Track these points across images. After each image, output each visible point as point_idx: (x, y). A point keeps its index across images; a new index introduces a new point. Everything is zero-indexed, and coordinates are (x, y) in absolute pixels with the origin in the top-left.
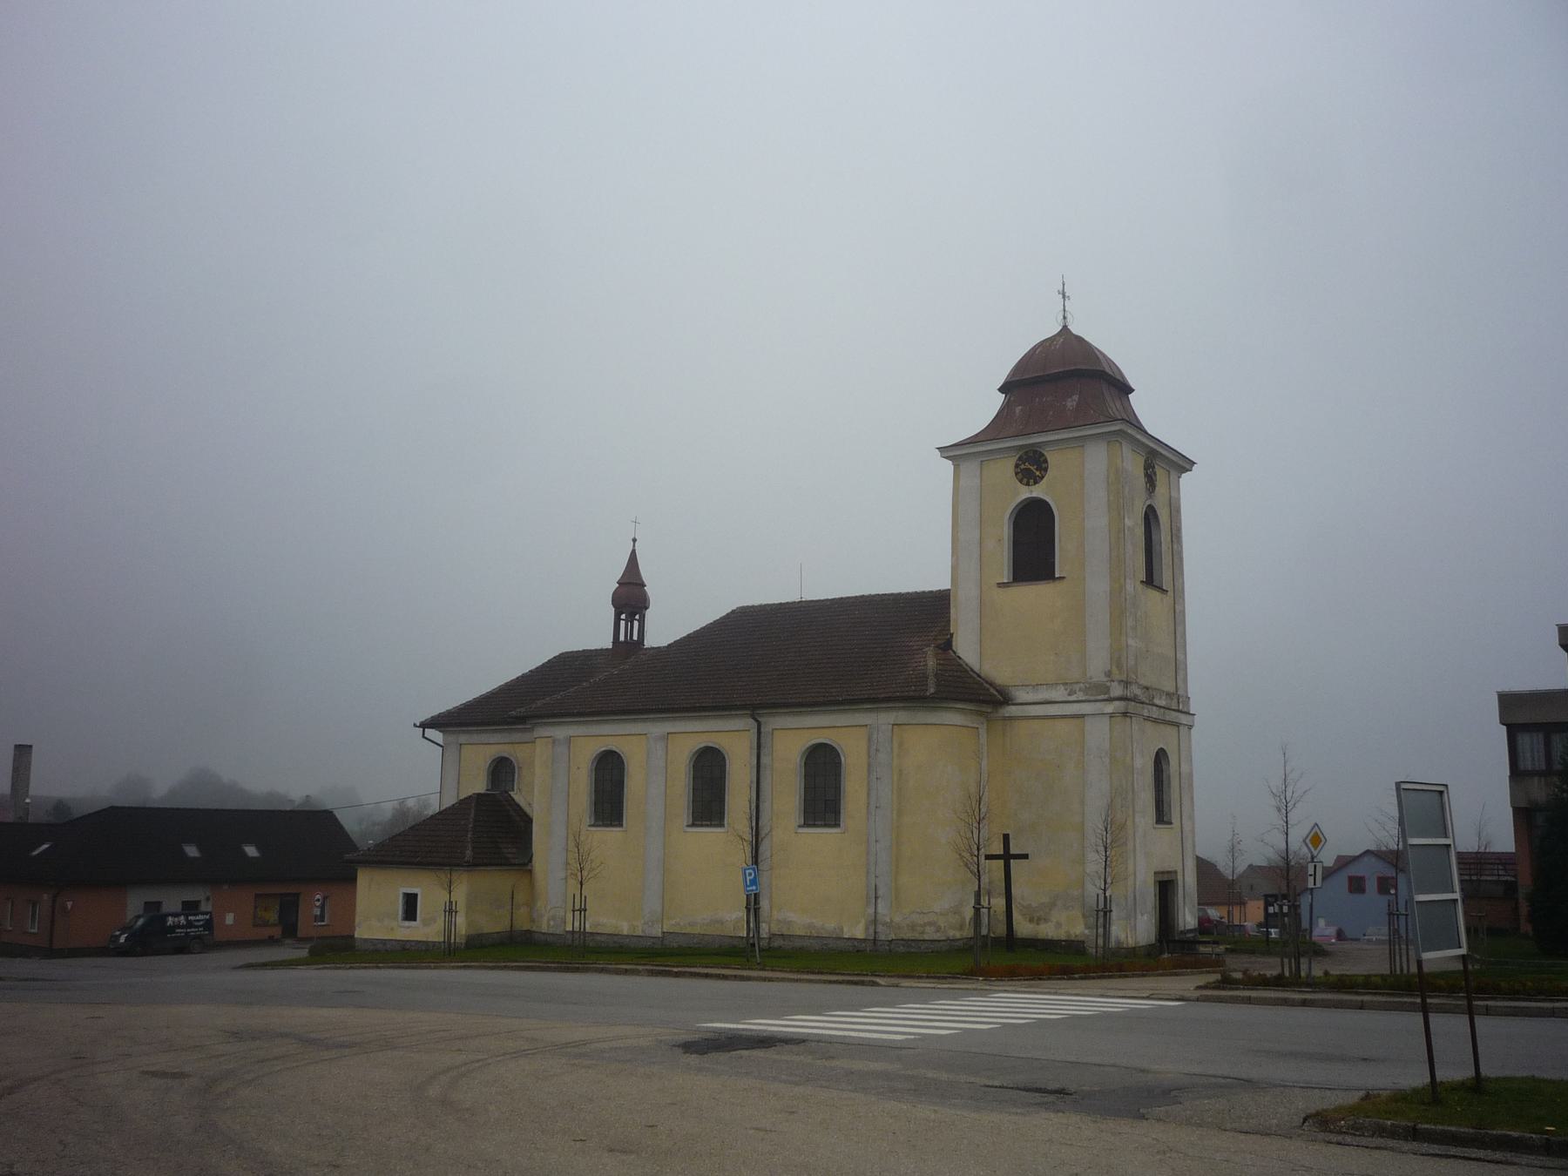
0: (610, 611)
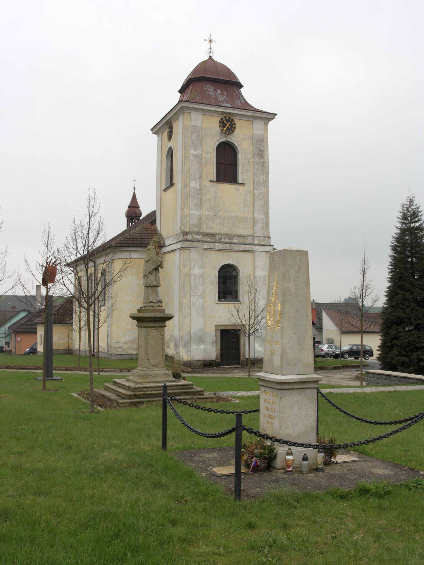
0: (125, 219)
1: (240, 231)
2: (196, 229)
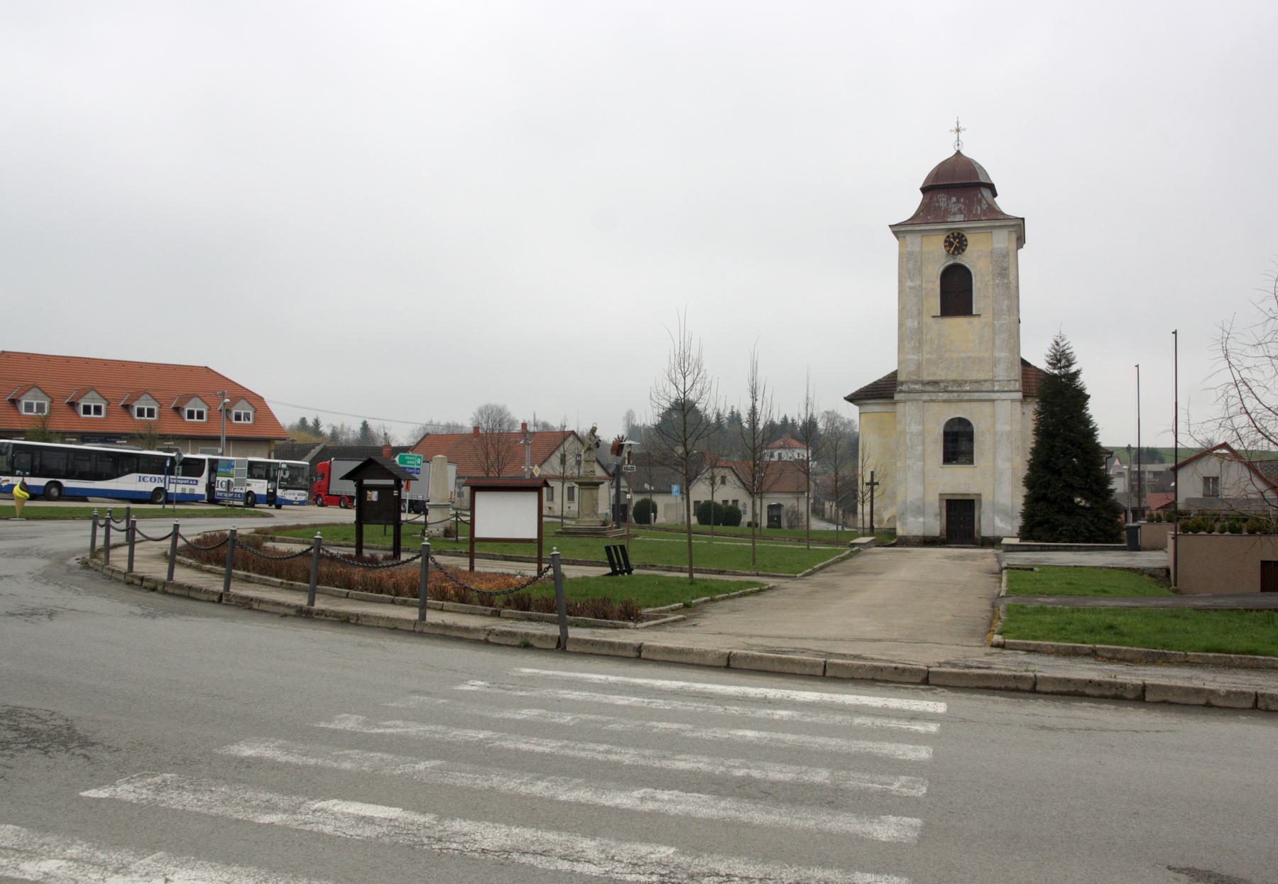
2: (914, 378)
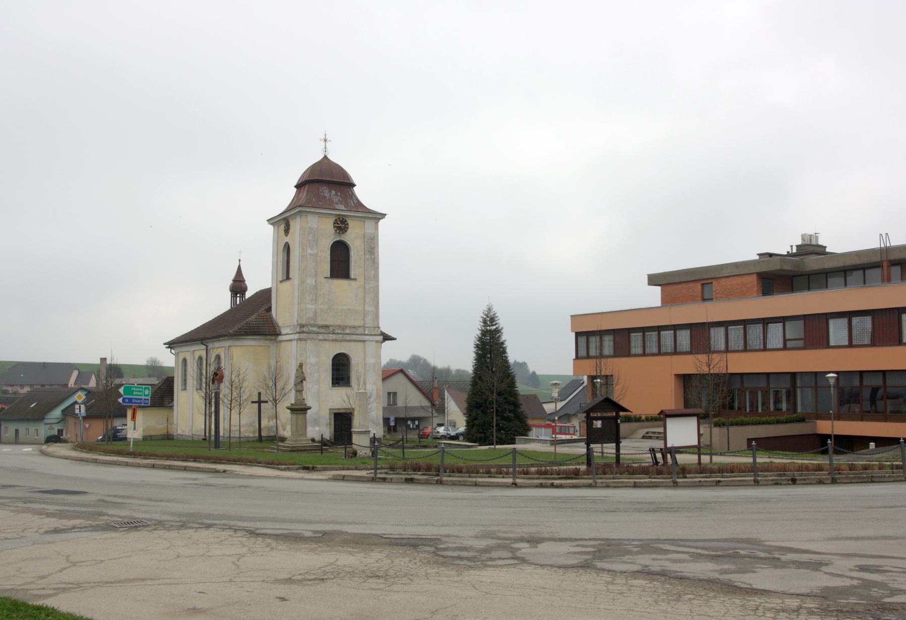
1: (352, 323)
